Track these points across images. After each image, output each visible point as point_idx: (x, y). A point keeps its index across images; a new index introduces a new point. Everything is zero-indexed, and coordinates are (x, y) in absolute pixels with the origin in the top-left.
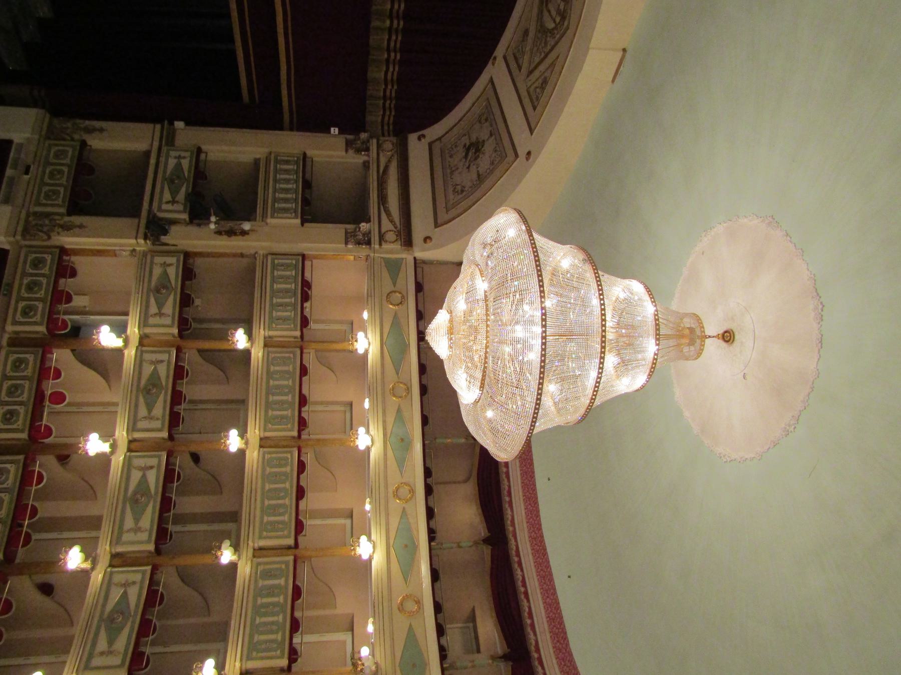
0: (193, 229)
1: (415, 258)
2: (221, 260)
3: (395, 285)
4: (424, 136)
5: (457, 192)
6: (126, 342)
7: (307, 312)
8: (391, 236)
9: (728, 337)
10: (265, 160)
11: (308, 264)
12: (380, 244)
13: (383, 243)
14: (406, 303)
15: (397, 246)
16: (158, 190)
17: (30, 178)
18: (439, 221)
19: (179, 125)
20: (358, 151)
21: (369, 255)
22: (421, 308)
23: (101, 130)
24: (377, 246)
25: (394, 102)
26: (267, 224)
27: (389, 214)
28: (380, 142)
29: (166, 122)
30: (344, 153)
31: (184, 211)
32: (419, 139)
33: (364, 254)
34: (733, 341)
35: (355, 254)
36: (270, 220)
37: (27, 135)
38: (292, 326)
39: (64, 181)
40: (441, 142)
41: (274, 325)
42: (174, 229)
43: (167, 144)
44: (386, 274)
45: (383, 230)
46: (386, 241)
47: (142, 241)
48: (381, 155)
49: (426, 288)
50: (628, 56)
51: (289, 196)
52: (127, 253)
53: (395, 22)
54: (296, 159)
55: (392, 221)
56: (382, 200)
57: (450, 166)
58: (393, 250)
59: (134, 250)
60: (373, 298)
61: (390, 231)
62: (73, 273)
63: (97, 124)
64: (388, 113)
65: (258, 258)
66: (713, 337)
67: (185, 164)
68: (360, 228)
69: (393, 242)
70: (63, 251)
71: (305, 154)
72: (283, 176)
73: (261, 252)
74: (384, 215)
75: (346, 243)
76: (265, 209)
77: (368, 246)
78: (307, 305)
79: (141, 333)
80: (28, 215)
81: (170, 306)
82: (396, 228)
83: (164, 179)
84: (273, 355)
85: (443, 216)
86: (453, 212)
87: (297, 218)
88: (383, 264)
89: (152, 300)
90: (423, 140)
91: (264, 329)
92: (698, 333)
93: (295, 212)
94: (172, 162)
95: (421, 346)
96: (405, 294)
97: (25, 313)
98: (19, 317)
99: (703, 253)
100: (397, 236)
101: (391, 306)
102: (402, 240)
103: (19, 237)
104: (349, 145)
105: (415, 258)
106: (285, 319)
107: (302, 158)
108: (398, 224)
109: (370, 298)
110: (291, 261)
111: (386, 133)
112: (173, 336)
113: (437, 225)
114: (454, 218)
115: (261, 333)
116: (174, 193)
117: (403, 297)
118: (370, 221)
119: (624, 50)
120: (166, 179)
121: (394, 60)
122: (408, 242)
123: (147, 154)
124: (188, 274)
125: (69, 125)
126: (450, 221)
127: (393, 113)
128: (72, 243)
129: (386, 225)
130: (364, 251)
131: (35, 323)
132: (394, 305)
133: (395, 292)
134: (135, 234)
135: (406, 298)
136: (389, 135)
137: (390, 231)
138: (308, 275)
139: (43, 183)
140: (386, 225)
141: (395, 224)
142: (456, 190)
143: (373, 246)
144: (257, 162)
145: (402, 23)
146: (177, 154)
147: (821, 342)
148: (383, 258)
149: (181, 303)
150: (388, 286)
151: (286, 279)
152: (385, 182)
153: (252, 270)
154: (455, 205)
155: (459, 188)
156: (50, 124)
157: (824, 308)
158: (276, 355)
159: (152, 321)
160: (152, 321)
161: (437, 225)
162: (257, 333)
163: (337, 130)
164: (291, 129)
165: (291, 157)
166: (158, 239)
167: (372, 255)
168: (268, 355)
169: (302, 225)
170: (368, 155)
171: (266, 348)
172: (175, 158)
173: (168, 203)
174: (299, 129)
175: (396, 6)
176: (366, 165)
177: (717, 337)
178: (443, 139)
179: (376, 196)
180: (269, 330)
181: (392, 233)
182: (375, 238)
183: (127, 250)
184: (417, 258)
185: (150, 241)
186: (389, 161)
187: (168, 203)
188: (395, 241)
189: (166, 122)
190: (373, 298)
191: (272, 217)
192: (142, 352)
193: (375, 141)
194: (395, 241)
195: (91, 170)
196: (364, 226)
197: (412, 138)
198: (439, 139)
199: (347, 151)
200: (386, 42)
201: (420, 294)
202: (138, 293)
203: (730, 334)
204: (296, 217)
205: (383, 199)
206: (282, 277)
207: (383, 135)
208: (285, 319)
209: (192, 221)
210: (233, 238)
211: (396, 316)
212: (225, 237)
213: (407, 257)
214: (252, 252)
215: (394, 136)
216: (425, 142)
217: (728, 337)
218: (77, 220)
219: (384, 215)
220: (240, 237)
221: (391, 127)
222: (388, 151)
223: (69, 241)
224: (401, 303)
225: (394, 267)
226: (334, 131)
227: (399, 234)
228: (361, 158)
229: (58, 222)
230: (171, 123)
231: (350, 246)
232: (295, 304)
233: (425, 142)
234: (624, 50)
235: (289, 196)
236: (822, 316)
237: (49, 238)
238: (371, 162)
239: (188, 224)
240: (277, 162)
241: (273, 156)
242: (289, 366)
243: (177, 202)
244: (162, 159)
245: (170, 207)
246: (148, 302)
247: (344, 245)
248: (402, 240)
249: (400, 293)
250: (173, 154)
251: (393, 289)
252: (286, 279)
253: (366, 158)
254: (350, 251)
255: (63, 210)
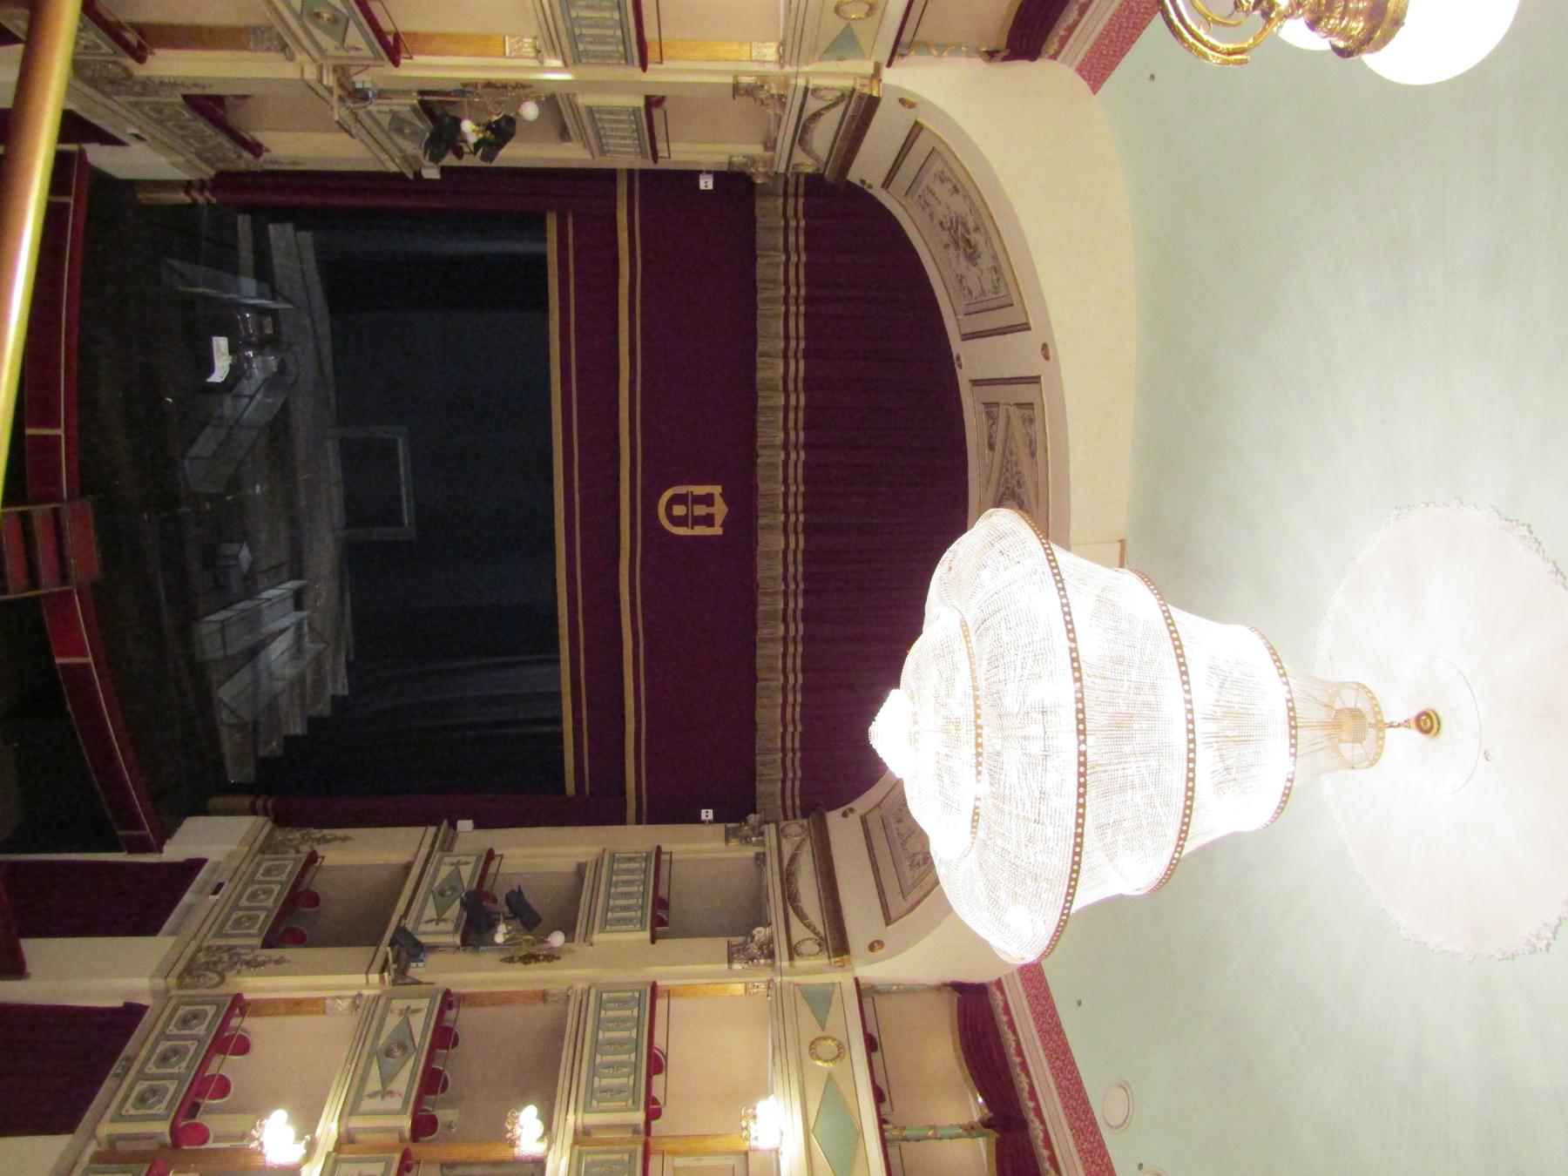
0: (465, 957)
1: (856, 980)
2: (507, 1012)
3: (823, 1029)
4: (852, 810)
5: (918, 864)
6: (311, 1147)
7: (657, 1092)
8: (810, 947)
9: (1427, 723)
10: (594, 865)
11: (661, 1004)
12: (791, 958)
13: (796, 957)
14: (848, 1055)
15: (823, 961)
16: (416, 906)
17: (218, 900)
18: (893, 913)
19: (465, 825)
20: (745, 840)
21: (772, 980)
22: (872, 1029)
23: (345, 839)
24: (785, 964)
25: (799, 755)
26: (592, 944)
27: (802, 917)
28: (781, 826)
29: (445, 823)
30: (722, 845)
31: (455, 931)
32: (845, 815)
33: (765, 979)
34: (1438, 729)
35: (747, 980)
36: (597, 937)
37: (233, 847)
38: (630, 1102)
39: (270, 903)
40: (880, 808)
41: (595, 1103)
42: (432, 959)
43: (442, 849)
44: (804, 1008)
45: (795, 940)
46: (800, 955)
47: (375, 978)
48: (784, 841)
49: (886, 1041)
50: (1128, 551)
51: (632, 902)
52: (345, 1004)
53: (792, 627)
54: (637, 994)
55: (808, 926)
56: (789, 899)
57: (899, 834)
58: (815, 970)
59: (360, 995)
60: (783, 1050)
61: (807, 939)
62: (243, 1046)
63: (340, 832)
64: (790, 729)
65: (572, 998)
66: (1399, 725)
67: (466, 872)
68: (753, 937)
69: (814, 955)
70: (239, 1005)
71: (659, 848)
72: (618, 902)
73: (579, 987)
74: (793, 919)
75: (730, 961)
76: (597, 879)
77: (769, 961)
78: (658, 1080)
79: (342, 1130)
80: (199, 950)
81: (406, 1078)
82: (814, 931)
83: (430, 891)
84: (589, 1158)
85: (896, 904)
86: (911, 899)
87: (645, 930)
88: (799, 995)
89: (375, 1070)
90: (851, 816)
91: (575, 1111)
92: (1370, 719)
93: (641, 922)
94: (445, 871)
95: (887, 1134)
96: (843, 1039)
97: (142, 1100)
98: (129, 1109)
99: (1331, 658)
100: (820, 945)
101: (819, 1063)
102: (830, 950)
103: (172, 981)
104: (729, 835)
105: (856, 980)
106: (616, 1092)
107: (654, 853)
108: (820, 928)
109: (777, 1052)
110: (630, 994)
111: (790, 814)
112: (401, 1133)
113: (888, 920)
114: (918, 903)
115: (570, 1121)
116: (441, 910)
117: (840, 1046)
118: (771, 924)
119: (1122, 541)
120: (432, 892)
121: (794, 686)
122: (837, 943)
123: (408, 867)
124: (444, 1037)
125: (298, 835)
126: (912, 908)
127: (799, 728)
128: (255, 990)
129: (799, 931)
130: (760, 977)
131: (153, 1118)
132: (826, 1061)
133: (825, 1038)
134: (366, 969)
135: (846, 1046)
136: (795, 817)
137: (807, 939)
138: (659, 1041)
139: (236, 907)
140: (799, 931)
141: (815, 929)
142: (916, 862)
143: (778, 964)
144: (581, 869)
145: (801, 626)
146: (455, 860)
147: (1558, 571)
148: (797, 984)
149: (422, 1084)
150: (810, 1029)
151: (619, 1023)
152: (794, 874)
153: (557, 1033)
154: (915, 885)
155: (919, 858)
156: (270, 836)
157: (1532, 528)
158: (596, 1157)
159: (367, 1105)
160: (367, 1105)
161: (888, 920)
162: (562, 1122)
163: (711, 812)
164: (639, 822)
165: (638, 853)
166: (402, 972)
167: (778, 979)
168: (579, 1162)
169: (653, 941)
170: (762, 843)
171: (577, 1147)
172: (452, 864)
173: (417, 1011)
174: (649, 822)
175: (792, 605)
176: (760, 859)
177: (1406, 724)
178: (882, 805)
179: (778, 892)
180: (585, 1111)
181: (809, 942)
182: (781, 948)
183: (348, 997)
184: (861, 981)
185: (390, 974)
186: (798, 848)
187: (417, 1011)
188: (818, 953)
189: (445, 823)
190: (783, 1050)
191: (602, 931)
192: (336, 1162)
193: (772, 827)
194: (818, 953)
195: (314, 899)
196: (760, 933)
197: (834, 818)
198: (878, 806)
199: (727, 841)
200: (779, 741)
201: (876, 1056)
202: (351, 1064)
203: (1431, 718)
204: (643, 929)
205: (791, 898)
206: (610, 1042)
207: (786, 818)
208: (616, 1092)
209: (465, 943)
210: (533, 965)
211: (830, 1077)
212: (519, 965)
213: (842, 979)
214: (564, 987)
215: (805, 816)
216: (854, 818)
217: (1427, 723)
218: (276, 953)
219: (793, 919)
220: (545, 964)
221: (797, 801)
222: (797, 836)
223: (254, 985)
224: (838, 1056)
225: (820, 1001)
226: (707, 814)
227: (822, 943)
228: (749, 852)
229: (243, 957)
230: (453, 825)
231: (737, 966)
232: (636, 1067)
233: (854, 818)
234: (1122, 541)
235: (632, 902)
236: (1536, 539)
237: (223, 978)
238: (768, 854)
239: (458, 948)
240: (600, 1005)
241: (607, 857)
242: (632, 1009)
243: (445, 920)
244: (431, 869)
245: (432, 927)
246: (366, 1072)
247: (726, 965)
248: (830, 950)
249: (834, 1040)
250: (447, 860)
251: (820, 1033)
252: (619, 1023)
253: (760, 849)
254: (738, 974)
255: (257, 941)
